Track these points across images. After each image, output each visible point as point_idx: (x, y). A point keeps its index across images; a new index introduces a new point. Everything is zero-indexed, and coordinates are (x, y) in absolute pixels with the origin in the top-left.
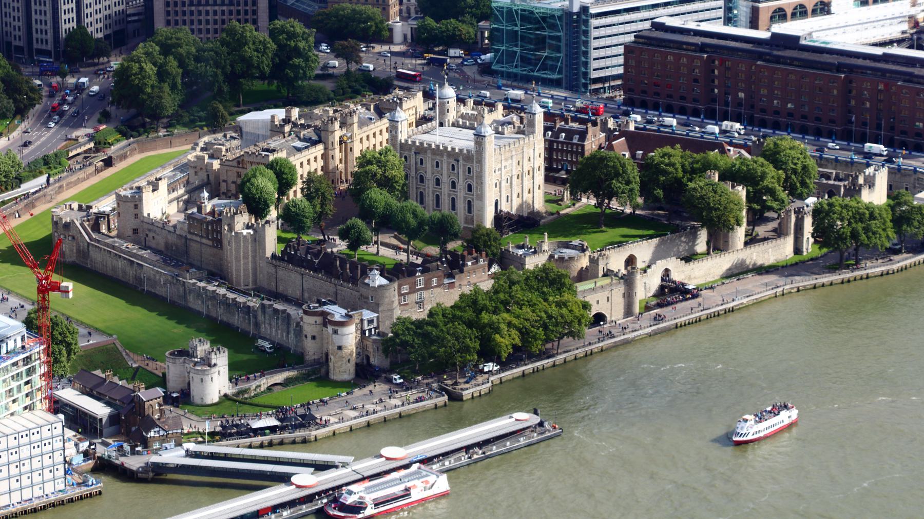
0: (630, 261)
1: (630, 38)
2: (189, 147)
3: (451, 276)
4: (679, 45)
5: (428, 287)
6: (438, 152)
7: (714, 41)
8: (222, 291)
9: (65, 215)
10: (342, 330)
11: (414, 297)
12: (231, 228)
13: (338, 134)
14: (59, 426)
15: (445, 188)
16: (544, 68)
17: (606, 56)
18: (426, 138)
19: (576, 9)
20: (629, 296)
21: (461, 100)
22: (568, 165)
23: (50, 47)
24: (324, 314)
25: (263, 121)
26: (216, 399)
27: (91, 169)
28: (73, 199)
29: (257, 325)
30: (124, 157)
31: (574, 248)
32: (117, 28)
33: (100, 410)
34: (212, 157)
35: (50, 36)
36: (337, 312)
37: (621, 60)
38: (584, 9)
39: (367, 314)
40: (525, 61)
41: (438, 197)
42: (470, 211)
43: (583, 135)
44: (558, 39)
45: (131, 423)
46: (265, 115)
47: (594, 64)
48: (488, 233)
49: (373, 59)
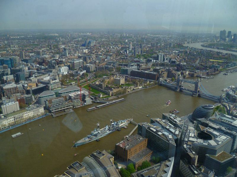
9: (91, 84)
17: (129, 72)
22: (126, 80)
36: (110, 91)
46: (105, 77)
49: (112, 72)
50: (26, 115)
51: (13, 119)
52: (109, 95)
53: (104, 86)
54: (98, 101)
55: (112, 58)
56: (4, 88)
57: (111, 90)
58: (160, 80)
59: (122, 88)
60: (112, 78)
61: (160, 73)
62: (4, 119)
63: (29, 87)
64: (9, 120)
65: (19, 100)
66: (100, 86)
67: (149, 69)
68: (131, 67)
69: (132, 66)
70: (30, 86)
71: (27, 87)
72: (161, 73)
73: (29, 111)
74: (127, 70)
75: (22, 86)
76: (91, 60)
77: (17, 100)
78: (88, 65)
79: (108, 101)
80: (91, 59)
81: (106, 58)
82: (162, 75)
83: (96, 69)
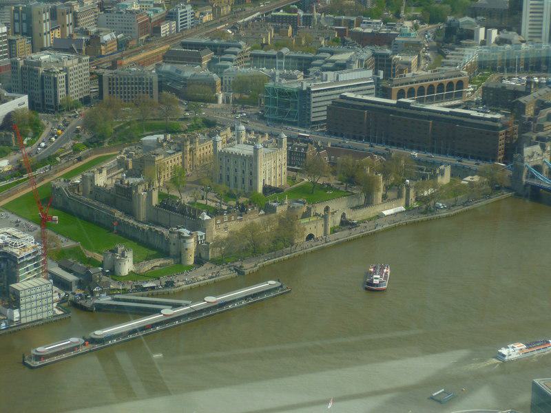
0: (327, 209)
1: (330, 103)
2: (118, 152)
3: (241, 216)
4: (354, 106)
5: (230, 220)
6: (237, 156)
7: (373, 105)
8: (131, 221)
9: (58, 184)
10: (188, 241)
11: (223, 225)
12: (137, 191)
13: (189, 147)
14: (50, 285)
15: (240, 173)
16: (289, 116)
17: (319, 112)
18: (230, 150)
19: (305, 88)
20: (325, 226)
21: (248, 131)
22: (295, 160)
23: (53, 103)
24: (180, 233)
25: (153, 141)
26: (127, 273)
27: (71, 163)
28: (62, 176)
29: (148, 238)
30: (87, 157)
31: (300, 202)
32: (86, 95)
33: (70, 277)
34: (128, 157)
35: (53, 96)
36: (186, 232)
37: (326, 113)
38: (309, 89)
39: (200, 233)
40: (281, 113)
41: (236, 178)
42: (251, 184)
43: (306, 148)
44: (296, 102)
45: (87, 282)
46: (154, 137)
47: (313, 115)
48: (259, 195)
49: (205, 112)
52: (179, 257)
53: (148, 196)
54: (105, 299)
55: (207, 18)
57: (197, 225)
58: (528, 163)
59: (269, 210)
60: (203, 149)
61: (530, 112)
66: (122, 196)
67: (453, 89)
68: (331, 75)
69: (342, 67)
72: (537, 112)
74: (305, 94)
76: (69, 30)
78: (44, 57)
79: (168, 295)
80: (69, 19)
81: (170, 17)
82: (541, 128)
83: (95, 88)
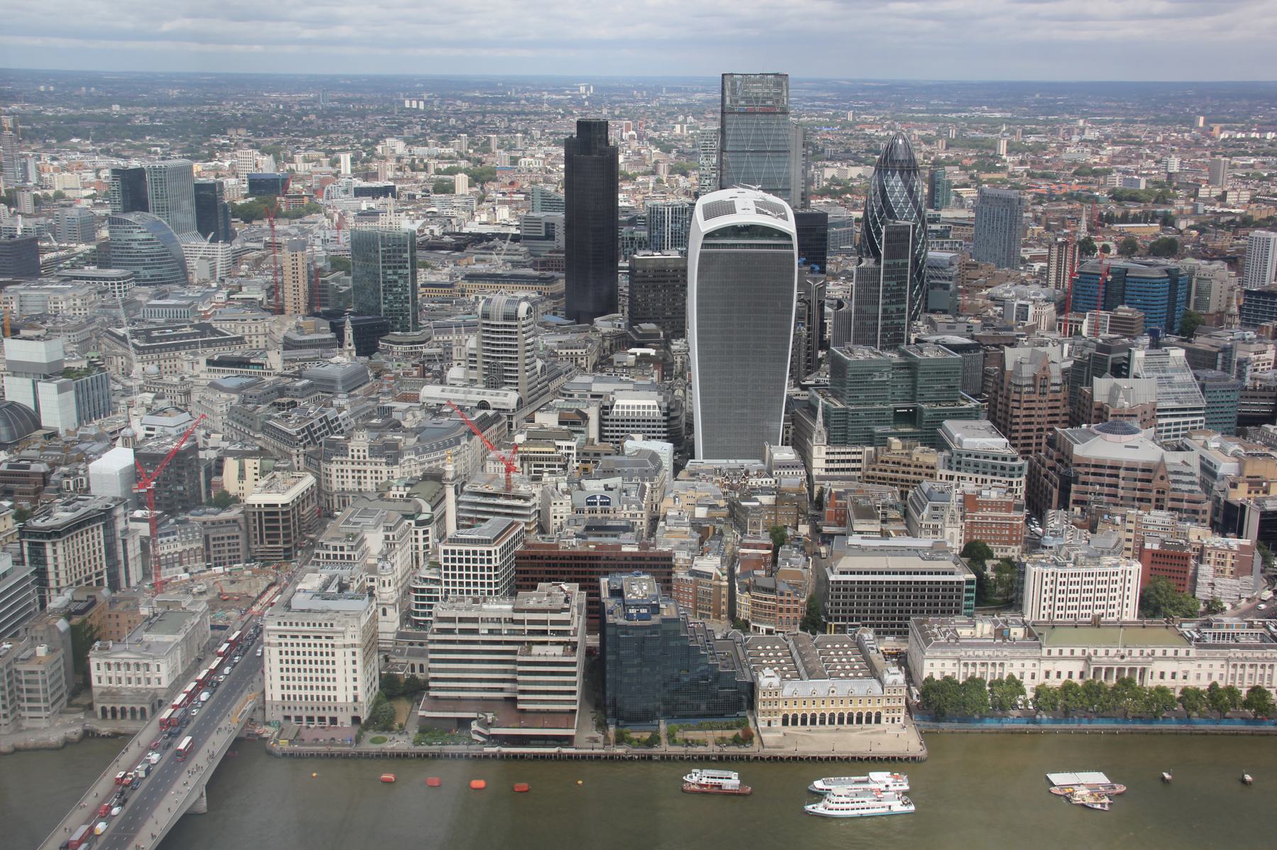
50: (1168, 667)
51: (1077, 667)
56: (1079, 450)
62: (1024, 646)
63: (1243, 487)
64: (1047, 665)
65: (1154, 554)
70: (1256, 484)
71: (1234, 486)
73: (1193, 652)
75: (1196, 469)
77: (1140, 554)
